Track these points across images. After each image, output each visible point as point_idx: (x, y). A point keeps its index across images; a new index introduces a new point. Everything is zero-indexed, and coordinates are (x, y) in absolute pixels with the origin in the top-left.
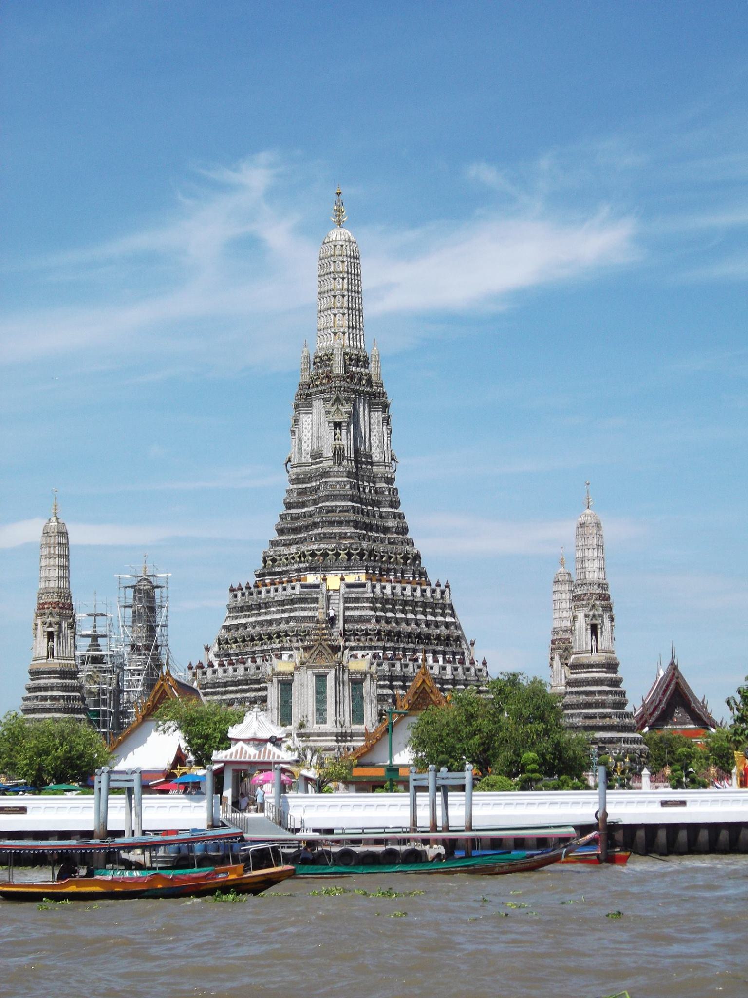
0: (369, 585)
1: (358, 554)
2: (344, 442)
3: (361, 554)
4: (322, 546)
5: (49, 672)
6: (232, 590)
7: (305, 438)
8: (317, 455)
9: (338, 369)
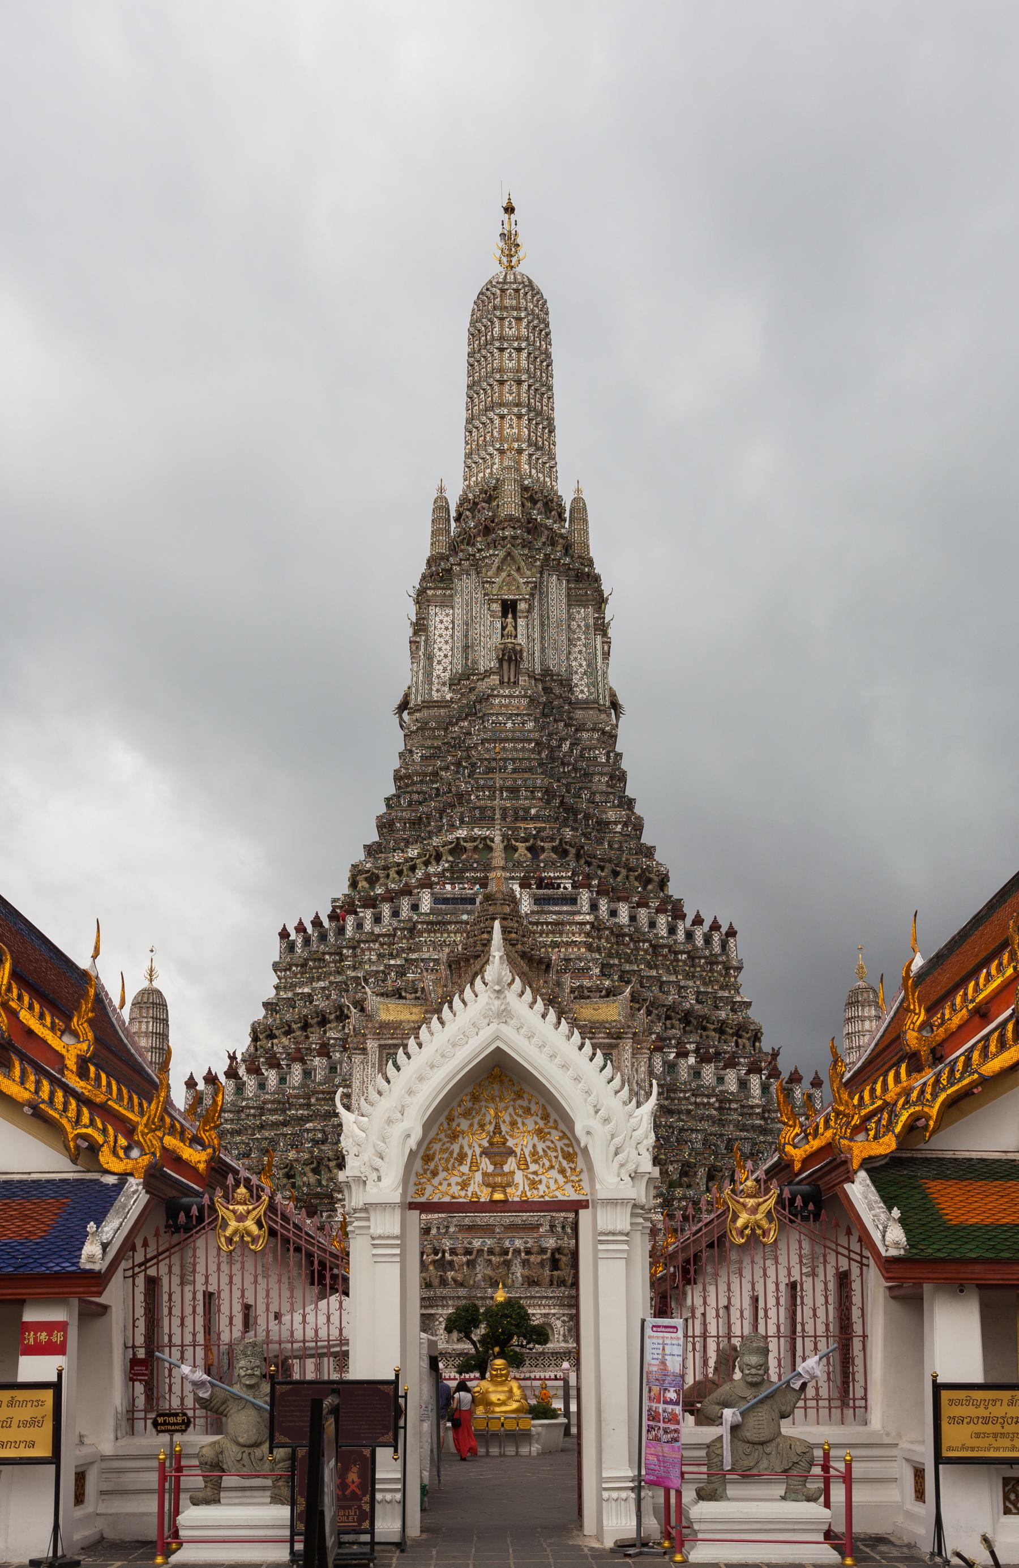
0: (585, 897)
1: (554, 849)
2: (521, 640)
4: (477, 831)
7: (439, 655)
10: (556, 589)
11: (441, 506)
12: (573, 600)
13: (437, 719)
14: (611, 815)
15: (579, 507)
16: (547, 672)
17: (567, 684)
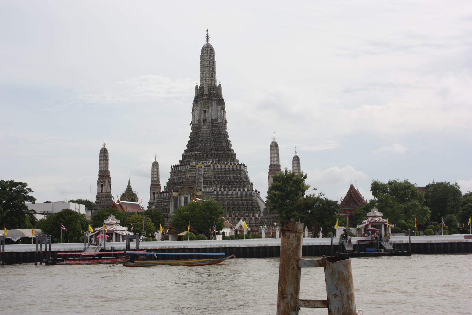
3: (211, 155)
5: (102, 197)
6: (171, 167)
8: (199, 121)
9: (206, 92)
10: (214, 104)
11: (197, 86)
12: (218, 104)
13: (196, 127)
14: (224, 144)
15: (220, 85)
16: (212, 120)
17: (217, 120)
